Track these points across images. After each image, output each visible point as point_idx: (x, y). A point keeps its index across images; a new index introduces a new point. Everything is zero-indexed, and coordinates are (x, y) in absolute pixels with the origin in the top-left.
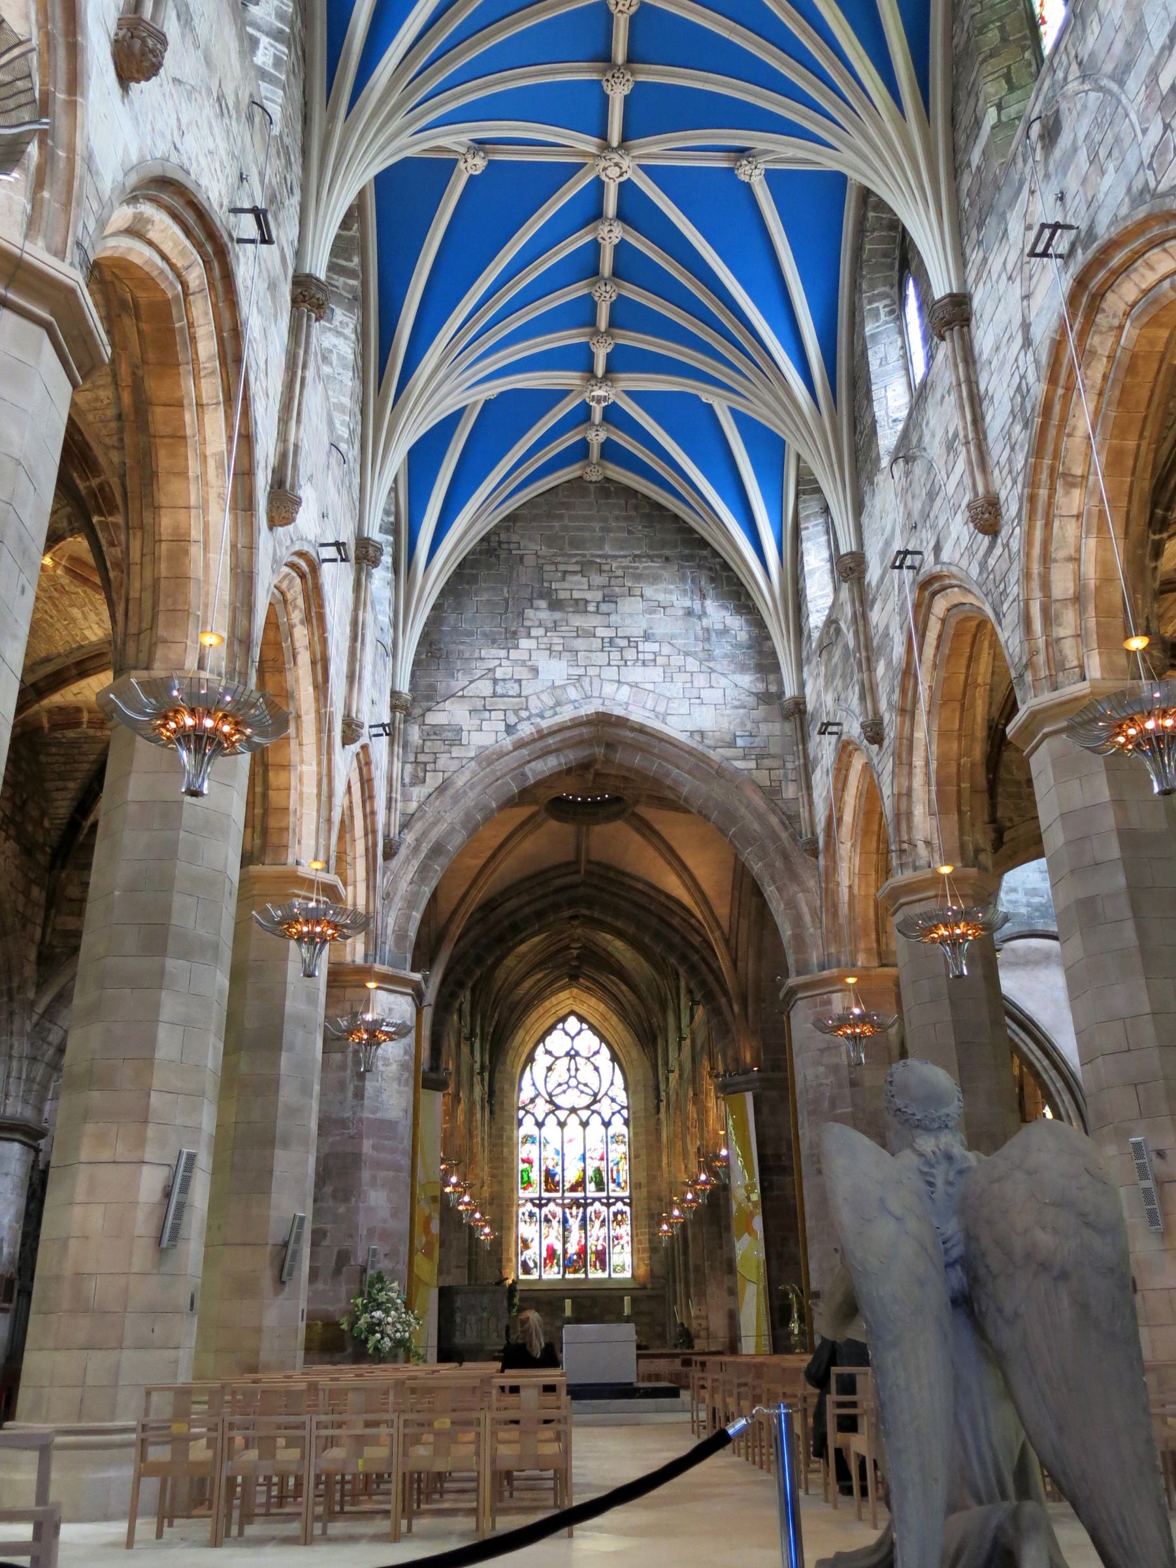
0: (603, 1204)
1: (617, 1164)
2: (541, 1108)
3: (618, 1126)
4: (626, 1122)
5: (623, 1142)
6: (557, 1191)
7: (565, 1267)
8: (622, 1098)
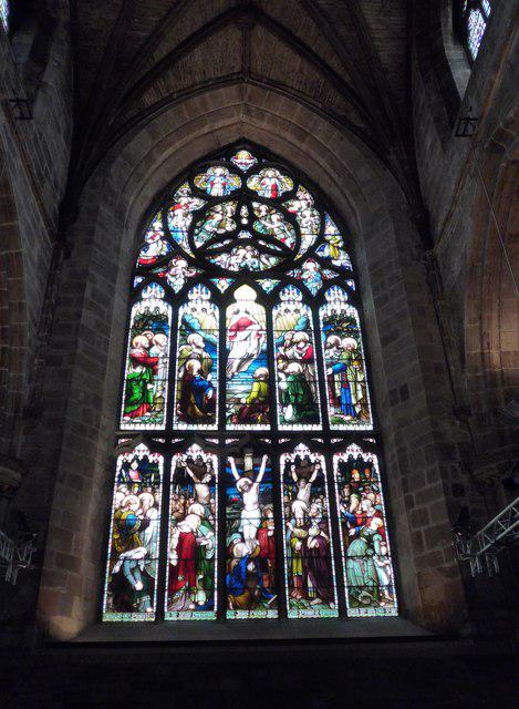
0: (314, 448)
1: (343, 370)
2: (179, 273)
3: (337, 303)
4: (355, 299)
5: (351, 333)
6: (213, 422)
7: (225, 591)
8: (342, 260)
